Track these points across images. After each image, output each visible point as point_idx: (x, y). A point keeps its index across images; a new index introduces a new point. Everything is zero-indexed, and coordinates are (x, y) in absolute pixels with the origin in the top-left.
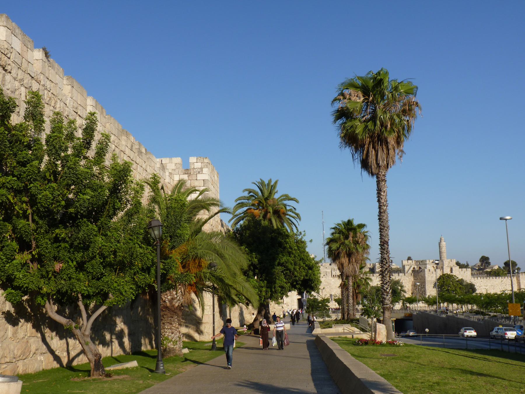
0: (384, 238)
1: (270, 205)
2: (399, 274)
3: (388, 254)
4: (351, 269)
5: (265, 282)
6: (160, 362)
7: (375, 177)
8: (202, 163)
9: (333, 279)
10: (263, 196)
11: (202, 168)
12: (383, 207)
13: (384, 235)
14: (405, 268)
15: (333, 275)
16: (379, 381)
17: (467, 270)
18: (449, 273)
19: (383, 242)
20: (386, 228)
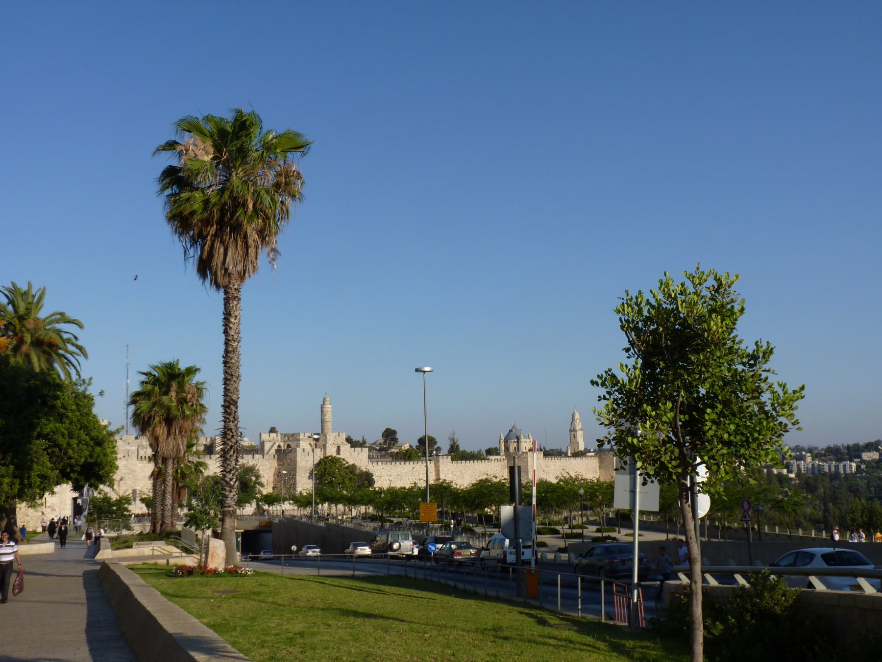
0: (230, 394)
1: (28, 330)
3: (236, 422)
4: (171, 447)
7: (222, 291)
9: (140, 463)
12: (232, 343)
13: (232, 390)
14: (264, 446)
15: (139, 457)
16: (205, 635)
18: (334, 454)
19: (229, 402)
20: (235, 379)
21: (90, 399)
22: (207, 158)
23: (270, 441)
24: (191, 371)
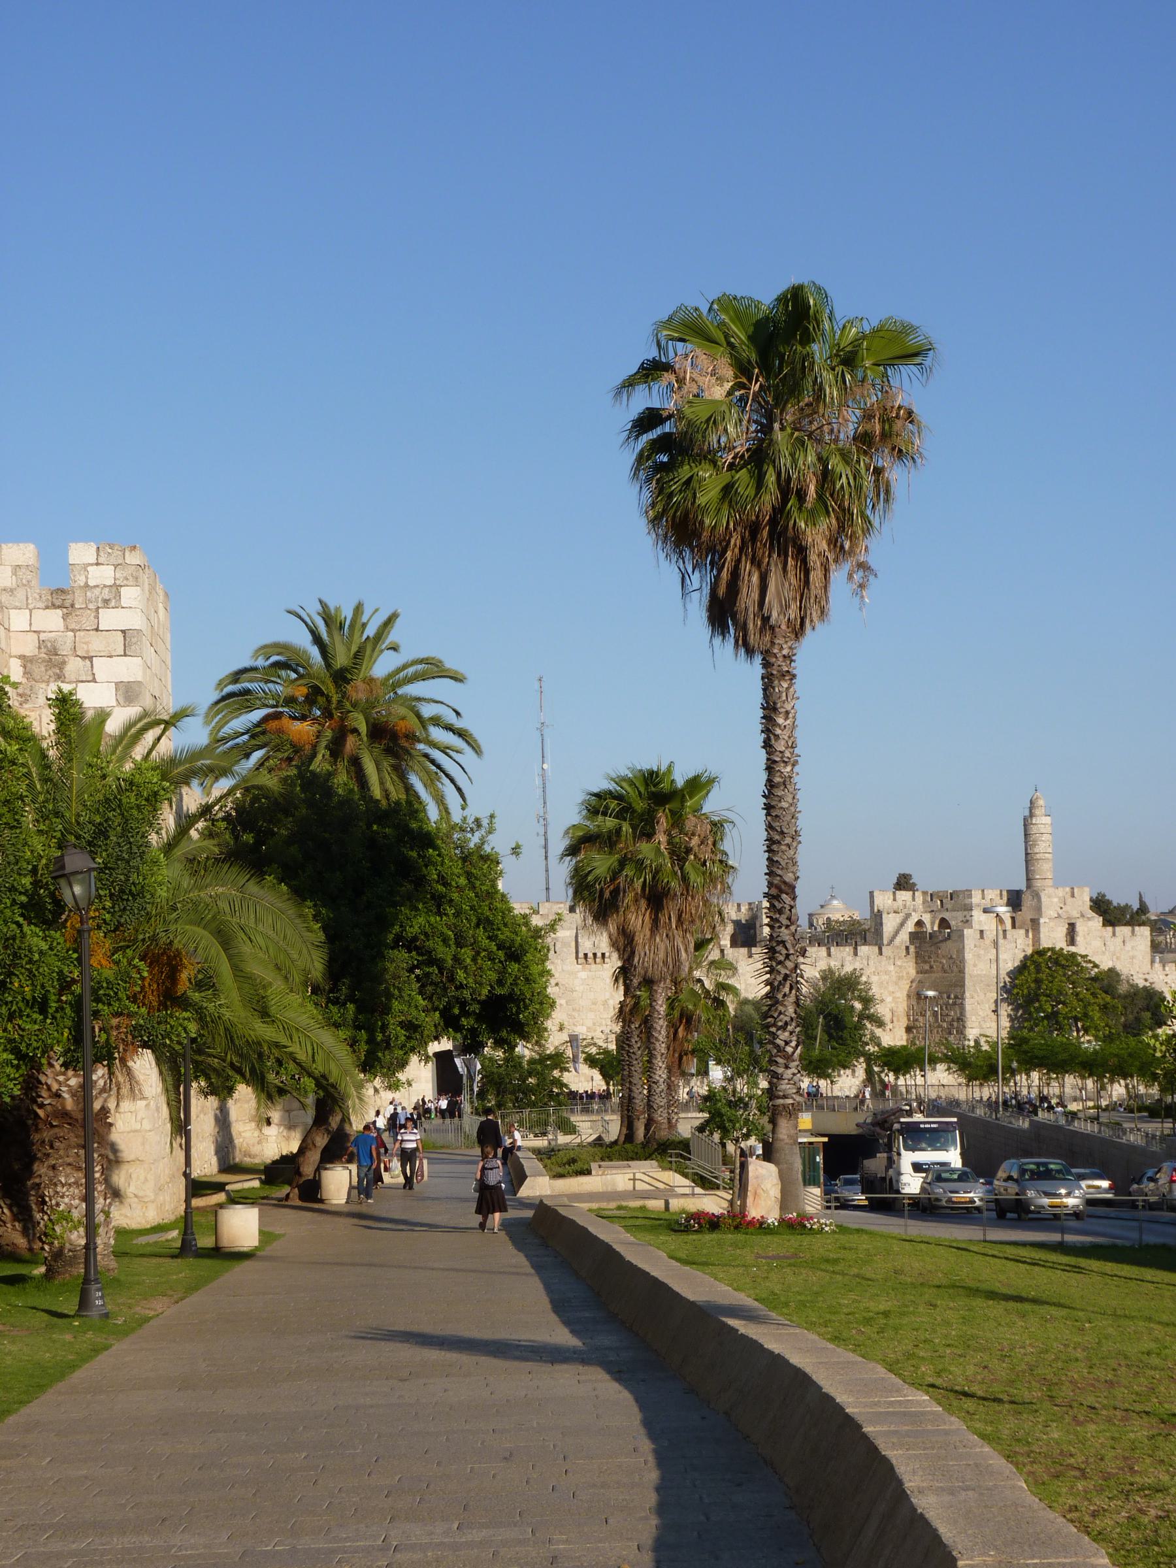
0: (779, 872)
1: (354, 705)
2: (856, 949)
3: (793, 928)
4: (662, 955)
5: (351, 1007)
6: (94, 1287)
7: (758, 659)
8: (116, 566)
9: (583, 970)
10: (328, 665)
11: (116, 588)
12: (780, 767)
13: (783, 863)
14: (881, 924)
15: (581, 955)
16: (741, 1303)
17: (1133, 932)
19: (777, 887)
20: (788, 840)
21: (491, 860)
22: (718, 392)
23: (895, 912)
24: (698, 785)
